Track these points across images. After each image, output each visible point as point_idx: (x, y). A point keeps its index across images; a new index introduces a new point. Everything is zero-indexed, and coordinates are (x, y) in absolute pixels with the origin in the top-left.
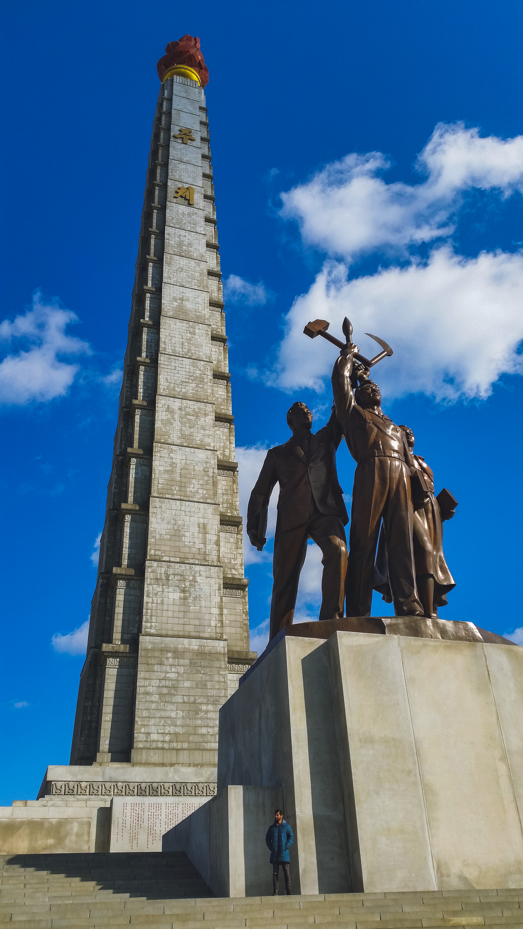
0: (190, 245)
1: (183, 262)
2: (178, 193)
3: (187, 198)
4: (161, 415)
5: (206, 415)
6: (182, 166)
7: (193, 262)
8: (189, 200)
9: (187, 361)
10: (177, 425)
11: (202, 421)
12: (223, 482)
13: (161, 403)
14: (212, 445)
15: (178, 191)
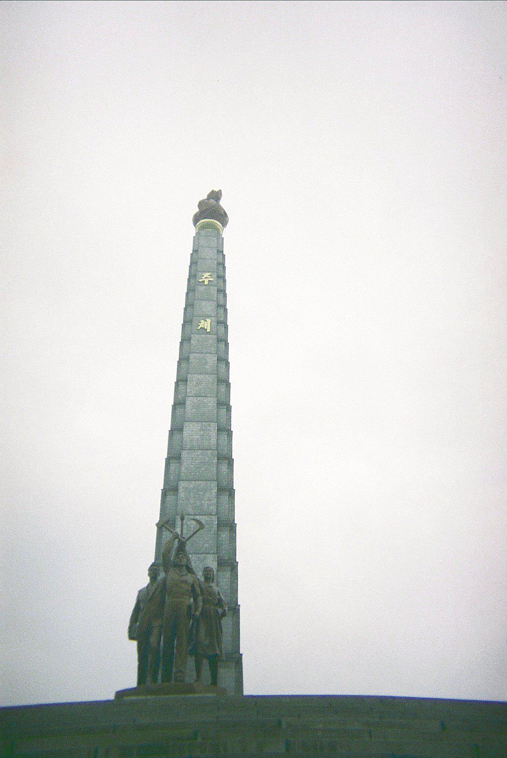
0: (206, 363)
1: (200, 377)
2: (199, 325)
3: (205, 328)
4: (182, 494)
5: (211, 489)
6: (204, 303)
7: (207, 376)
8: (206, 329)
9: (199, 452)
10: (192, 501)
11: (207, 495)
12: (223, 536)
13: (182, 485)
14: (215, 510)
15: (199, 324)
